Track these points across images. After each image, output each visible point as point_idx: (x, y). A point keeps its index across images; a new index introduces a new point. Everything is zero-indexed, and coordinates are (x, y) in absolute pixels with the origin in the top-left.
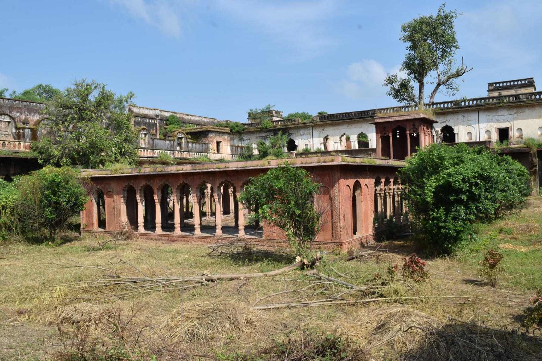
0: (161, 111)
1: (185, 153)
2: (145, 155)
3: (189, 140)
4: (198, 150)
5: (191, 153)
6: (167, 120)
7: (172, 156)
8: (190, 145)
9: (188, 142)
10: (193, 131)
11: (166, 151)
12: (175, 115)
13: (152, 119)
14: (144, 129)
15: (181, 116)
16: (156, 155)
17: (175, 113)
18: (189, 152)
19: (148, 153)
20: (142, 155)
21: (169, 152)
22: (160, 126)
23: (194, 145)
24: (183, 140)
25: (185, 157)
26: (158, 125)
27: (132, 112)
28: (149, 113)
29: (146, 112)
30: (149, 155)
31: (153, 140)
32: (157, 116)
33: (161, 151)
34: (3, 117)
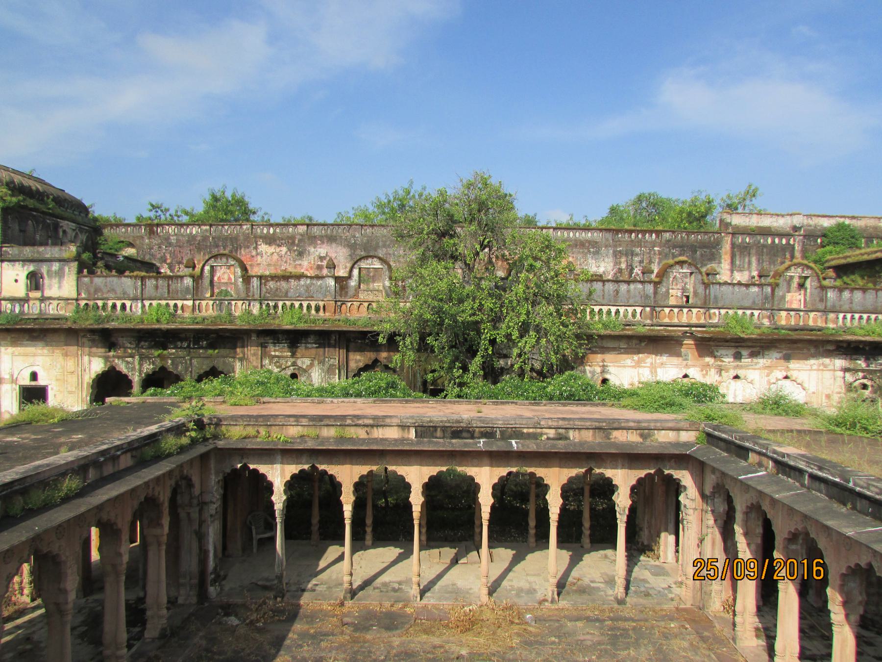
0: (809, 216)
1: (812, 315)
2: (684, 320)
3: (826, 283)
4: (855, 307)
5: (832, 316)
6: (824, 236)
7: (766, 322)
8: (831, 294)
9: (823, 288)
10: (866, 258)
11: (748, 312)
12: (847, 222)
13: (781, 235)
14: (681, 263)
15: (871, 223)
16: (715, 320)
17: (853, 218)
18: (825, 311)
19: (694, 316)
20: (675, 321)
21: (756, 313)
22: (804, 251)
23: (846, 294)
24: (808, 283)
25: (811, 323)
26: (797, 247)
27: (728, 225)
28: (775, 224)
29: (766, 222)
30: (694, 321)
31: (706, 286)
32: (795, 229)
33: (731, 312)
34: (370, 261)
